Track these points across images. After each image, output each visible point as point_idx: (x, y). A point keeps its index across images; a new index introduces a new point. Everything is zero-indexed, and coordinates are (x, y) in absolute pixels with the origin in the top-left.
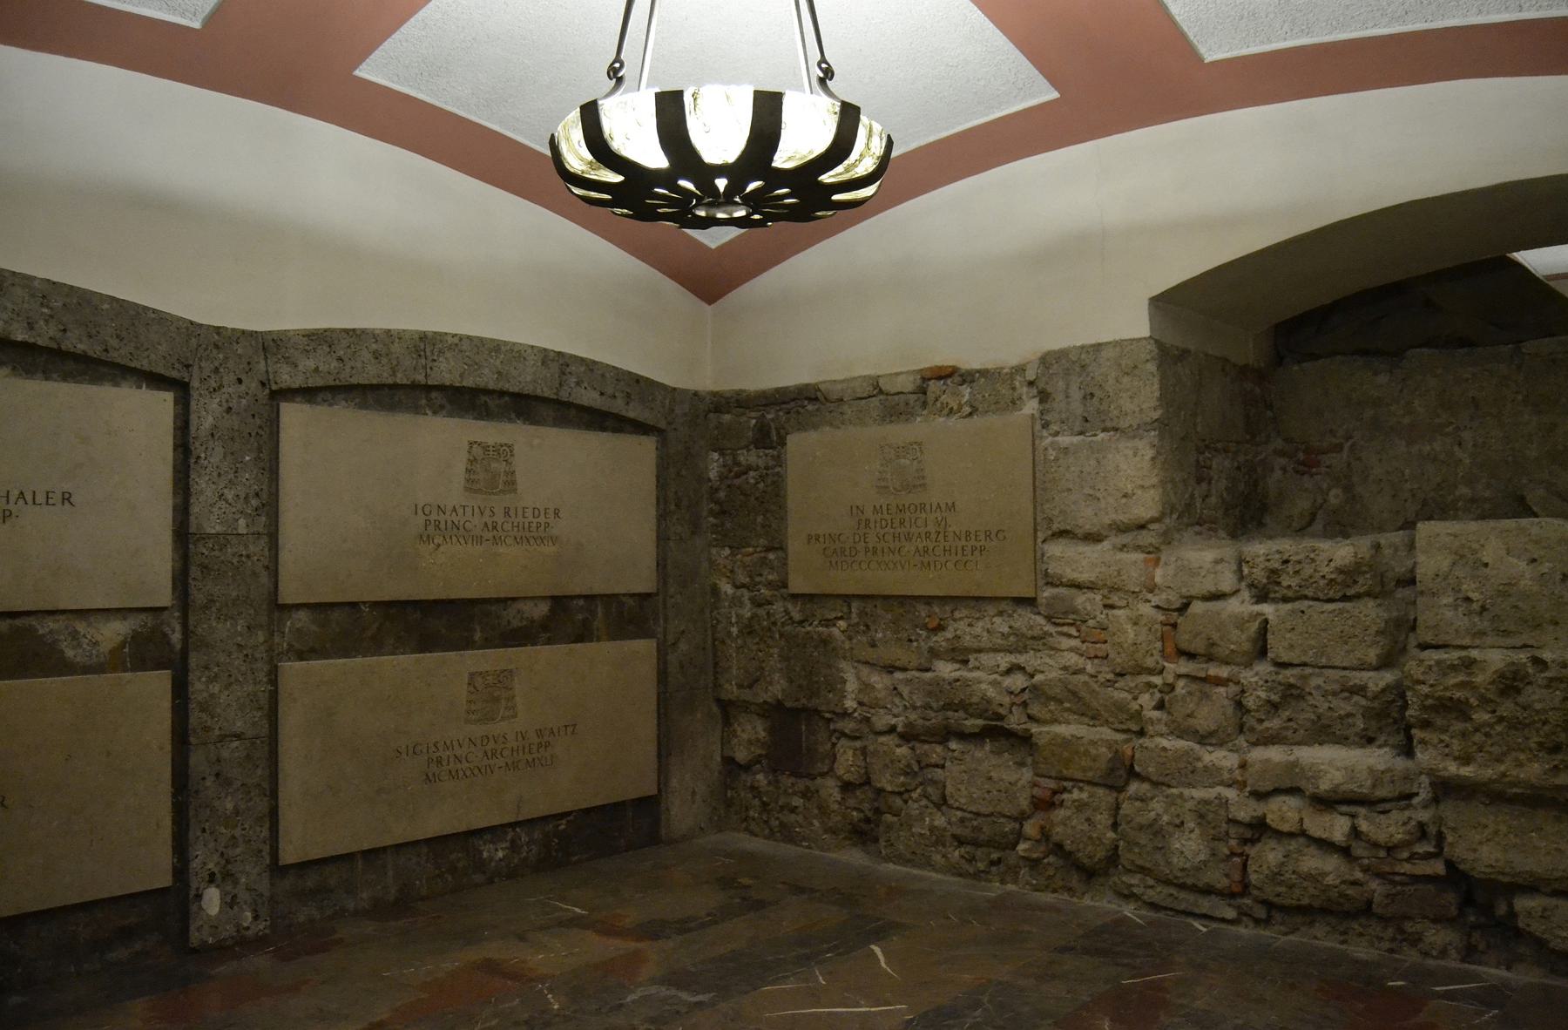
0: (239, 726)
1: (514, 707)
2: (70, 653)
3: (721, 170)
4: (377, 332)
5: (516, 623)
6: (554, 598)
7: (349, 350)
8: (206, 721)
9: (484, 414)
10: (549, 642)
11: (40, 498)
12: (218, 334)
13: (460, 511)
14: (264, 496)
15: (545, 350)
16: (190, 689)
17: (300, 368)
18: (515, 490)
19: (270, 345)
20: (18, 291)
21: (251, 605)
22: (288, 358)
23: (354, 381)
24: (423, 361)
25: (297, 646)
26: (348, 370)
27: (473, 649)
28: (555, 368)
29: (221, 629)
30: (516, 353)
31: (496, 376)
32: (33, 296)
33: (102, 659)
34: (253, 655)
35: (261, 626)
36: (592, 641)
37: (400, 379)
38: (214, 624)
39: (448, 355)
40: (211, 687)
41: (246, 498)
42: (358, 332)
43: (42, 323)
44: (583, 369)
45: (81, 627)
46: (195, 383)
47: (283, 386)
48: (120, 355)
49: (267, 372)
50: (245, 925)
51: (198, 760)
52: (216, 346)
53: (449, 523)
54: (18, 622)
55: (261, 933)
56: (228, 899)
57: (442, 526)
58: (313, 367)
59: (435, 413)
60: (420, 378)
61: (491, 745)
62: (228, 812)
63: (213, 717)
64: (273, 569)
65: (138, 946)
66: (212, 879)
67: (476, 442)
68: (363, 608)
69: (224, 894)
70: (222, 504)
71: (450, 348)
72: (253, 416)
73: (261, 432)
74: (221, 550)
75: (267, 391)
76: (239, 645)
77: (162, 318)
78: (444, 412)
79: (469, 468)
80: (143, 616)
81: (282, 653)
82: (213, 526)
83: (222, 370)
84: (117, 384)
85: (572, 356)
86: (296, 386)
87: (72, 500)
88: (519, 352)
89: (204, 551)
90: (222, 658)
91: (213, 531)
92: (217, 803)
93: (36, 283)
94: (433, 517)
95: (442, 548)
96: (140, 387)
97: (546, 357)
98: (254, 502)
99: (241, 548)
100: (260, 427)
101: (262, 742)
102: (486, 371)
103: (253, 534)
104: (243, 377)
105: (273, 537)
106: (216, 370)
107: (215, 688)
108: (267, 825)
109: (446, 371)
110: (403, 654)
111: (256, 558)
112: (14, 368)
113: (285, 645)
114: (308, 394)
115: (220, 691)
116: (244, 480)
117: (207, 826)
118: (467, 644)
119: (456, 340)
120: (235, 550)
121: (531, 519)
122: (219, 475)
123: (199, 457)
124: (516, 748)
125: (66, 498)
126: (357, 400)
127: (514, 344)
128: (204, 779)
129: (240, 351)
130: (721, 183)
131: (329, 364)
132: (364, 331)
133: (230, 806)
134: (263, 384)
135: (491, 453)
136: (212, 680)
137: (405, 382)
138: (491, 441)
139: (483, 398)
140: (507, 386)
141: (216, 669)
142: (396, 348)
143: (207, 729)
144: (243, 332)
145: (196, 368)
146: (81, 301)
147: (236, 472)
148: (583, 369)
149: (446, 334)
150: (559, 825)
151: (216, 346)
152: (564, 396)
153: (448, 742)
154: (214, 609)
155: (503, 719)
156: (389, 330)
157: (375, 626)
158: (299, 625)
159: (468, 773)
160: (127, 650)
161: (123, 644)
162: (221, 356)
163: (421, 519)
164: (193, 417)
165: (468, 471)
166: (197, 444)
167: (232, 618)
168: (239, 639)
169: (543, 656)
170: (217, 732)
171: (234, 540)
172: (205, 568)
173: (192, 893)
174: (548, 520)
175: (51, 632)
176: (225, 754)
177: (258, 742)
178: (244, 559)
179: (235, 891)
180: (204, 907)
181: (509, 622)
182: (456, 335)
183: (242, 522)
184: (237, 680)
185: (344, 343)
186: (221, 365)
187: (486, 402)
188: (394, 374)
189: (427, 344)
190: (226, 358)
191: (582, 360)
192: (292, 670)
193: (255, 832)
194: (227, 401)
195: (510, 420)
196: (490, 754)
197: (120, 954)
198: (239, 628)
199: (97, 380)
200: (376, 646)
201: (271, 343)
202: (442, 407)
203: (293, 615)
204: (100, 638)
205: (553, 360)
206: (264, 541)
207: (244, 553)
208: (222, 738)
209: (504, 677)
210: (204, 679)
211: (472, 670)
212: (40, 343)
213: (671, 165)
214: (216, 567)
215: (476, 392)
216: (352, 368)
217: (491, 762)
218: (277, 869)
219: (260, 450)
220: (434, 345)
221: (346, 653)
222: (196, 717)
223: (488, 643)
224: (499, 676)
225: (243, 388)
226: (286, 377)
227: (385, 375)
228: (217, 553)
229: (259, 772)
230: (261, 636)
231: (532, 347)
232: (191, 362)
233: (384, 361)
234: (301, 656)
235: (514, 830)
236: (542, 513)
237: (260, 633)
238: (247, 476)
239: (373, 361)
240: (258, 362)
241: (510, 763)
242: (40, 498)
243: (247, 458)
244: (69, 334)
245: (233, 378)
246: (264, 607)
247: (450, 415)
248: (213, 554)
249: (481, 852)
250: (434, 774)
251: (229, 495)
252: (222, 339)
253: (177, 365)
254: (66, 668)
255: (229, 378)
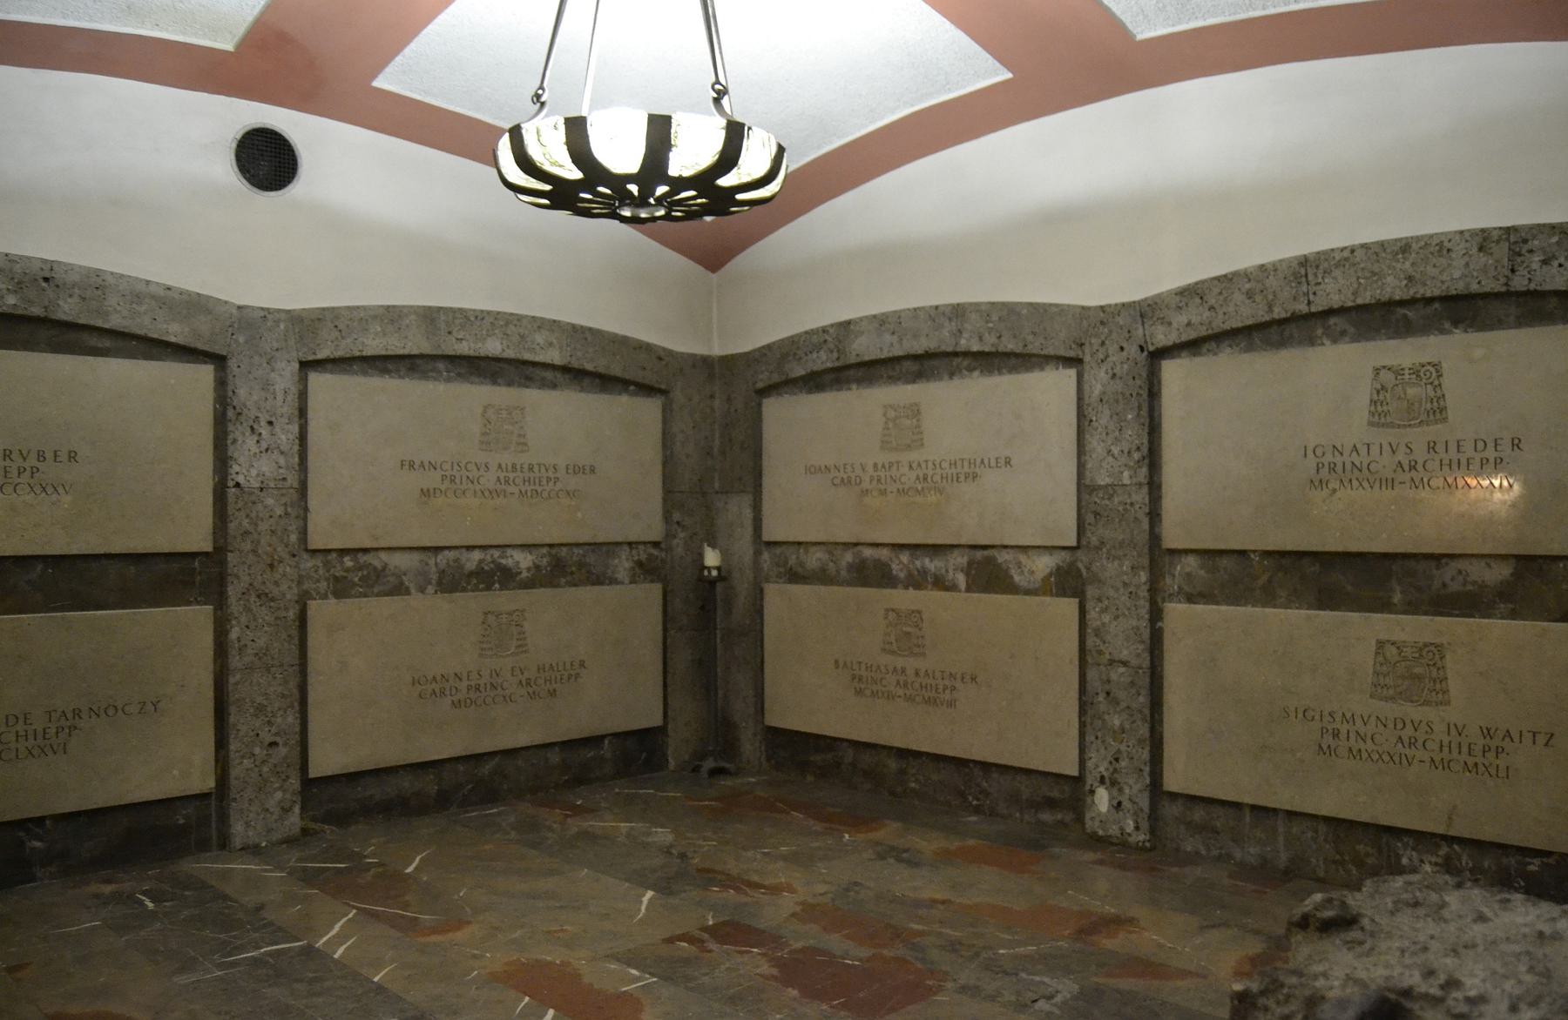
0: (1124, 654)
1: (1445, 692)
2: (1017, 578)
3: (629, 178)
4: (1249, 271)
5: (1455, 587)
6: (1518, 557)
7: (1221, 298)
8: (1099, 646)
9: (1405, 329)
10: (1514, 615)
11: (993, 463)
12: (1104, 312)
13: (1363, 451)
14: (1145, 450)
15: (1483, 231)
16: (1088, 617)
17: (1175, 325)
18: (1445, 420)
19: (1146, 311)
20: (974, 316)
21: (1134, 548)
22: (1163, 318)
23: (1227, 326)
24: (1304, 288)
25: (1186, 588)
26: (1221, 316)
27: (1390, 612)
28: (1501, 252)
29: (1111, 568)
30: (1439, 247)
31: (1405, 282)
32: (981, 316)
33: (1037, 586)
34: (1136, 593)
35: (1144, 568)
36: (926, 588)
37: (1278, 313)
38: (1105, 563)
39: (1337, 273)
40: (1103, 617)
41: (1129, 452)
42: (1230, 276)
43: (987, 335)
44: (1555, 239)
45: (1023, 558)
46: (1087, 358)
47: (1160, 345)
48: (1034, 348)
49: (1145, 335)
50: (1128, 831)
51: (1092, 674)
52: (1102, 323)
53: (1348, 467)
54: (986, 553)
55: (1140, 844)
56: (1115, 803)
57: (1339, 468)
58: (1186, 321)
59: (1335, 341)
60: (1302, 307)
61: (1409, 731)
62: (1116, 728)
63: (1104, 643)
64: (1154, 515)
65: (1059, 817)
66: (1102, 780)
67: (1384, 367)
68: (1252, 556)
69: (1111, 798)
70: (1110, 459)
71: (1337, 266)
72: (1134, 378)
73: (1141, 392)
74: (1109, 499)
75: (1146, 353)
76: (1125, 584)
77: (1062, 309)
78: (1347, 339)
79: (1375, 397)
80: (1063, 553)
81: (1173, 594)
82: (1103, 479)
83: (1107, 342)
84: (1042, 369)
85: (1532, 227)
86: (1171, 343)
87: (1521, 446)
88: (1441, 244)
89: (1096, 500)
90: (1111, 593)
91: (1102, 483)
92: (1106, 717)
93: (983, 308)
94: (1329, 458)
95: (1338, 494)
96: (1057, 369)
97: (1484, 240)
98: (1136, 456)
99: (1126, 496)
100: (1140, 387)
101: (1144, 672)
102: (1389, 279)
103: (1136, 484)
104: (1125, 345)
105: (1154, 487)
106: (1103, 343)
107: (1106, 618)
108: (1148, 748)
109: (1333, 292)
110: (1297, 608)
111: (1138, 506)
112: (981, 372)
113: (1176, 587)
114: (1193, 346)
115: (1110, 622)
116: (1127, 436)
117: (1099, 734)
118: (1385, 606)
119: (1346, 254)
120: (1121, 499)
121: (1470, 452)
122: (1107, 434)
123: (1091, 421)
124: (1445, 743)
125: (1008, 462)
126: (1242, 345)
127: (1431, 236)
128: (1097, 694)
129: (1121, 323)
130: (633, 188)
131: (1201, 315)
132: (1236, 274)
133: (1117, 722)
134: (1142, 349)
135: (1407, 376)
136: (1105, 610)
137: (1283, 315)
138: (1407, 362)
139: (1401, 311)
140: (1422, 291)
141: (1106, 603)
142: (1272, 282)
143: (1100, 652)
144: (1123, 305)
145: (1087, 344)
146: (1010, 311)
147: (1120, 430)
148: (1555, 239)
149: (1333, 250)
150: (1530, 864)
151: (1102, 323)
152: (1519, 283)
153: (1348, 715)
154: (1104, 550)
155: (1426, 703)
156: (1263, 265)
157: (1265, 578)
158: (1188, 570)
159: (1375, 757)
160: (1053, 579)
161: (1050, 574)
162: (1106, 330)
163: (1311, 462)
164: (1086, 387)
165: (1373, 402)
166: (1090, 409)
167: (1120, 559)
168: (1125, 577)
169: (1498, 631)
170: (1108, 656)
171: (1120, 491)
172: (1096, 514)
173: (1087, 787)
174: (1502, 455)
175: (1006, 561)
176: (1114, 676)
177: (1141, 671)
178: (1128, 507)
179: (1120, 798)
180: (1096, 802)
181: (1444, 585)
182: (1346, 248)
183: (1126, 474)
184: (1124, 614)
185: (1216, 290)
186: (1106, 338)
187: (1405, 316)
188: (1270, 308)
189: (1306, 268)
190: (1111, 332)
191: (1553, 227)
192: (1176, 611)
193: (1137, 751)
194: (1112, 369)
195: (1443, 332)
196: (1406, 741)
197: (1046, 816)
198: (1125, 568)
199: (1029, 369)
200: (1268, 598)
201: (1147, 309)
202: (1343, 333)
203: (1183, 560)
204: (1034, 568)
205: (1498, 242)
206: (1145, 490)
207: (1129, 501)
208: (1112, 662)
209: (1433, 652)
210: (1097, 609)
211: (1383, 636)
212: (987, 350)
213: (669, 176)
214: (1106, 514)
215: (1390, 305)
216: (1225, 314)
217: (1407, 751)
218: (1156, 786)
219: (1140, 408)
220: (1317, 267)
221: (1235, 600)
222: (1091, 641)
223: (1412, 608)
224: (1421, 649)
225: (1125, 353)
226: (1161, 337)
227: (1261, 313)
228: (1107, 502)
229: (1141, 699)
230: (1143, 576)
231: (1462, 232)
232: (1083, 341)
233: (1258, 298)
234: (1191, 599)
235: (1450, 846)
236: (1491, 445)
237: (1142, 573)
238: (1130, 433)
239: (1247, 301)
240: (1136, 329)
241: (1437, 759)
242: (993, 463)
243: (1130, 416)
244: (1003, 339)
245: (1116, 347)
246: (1146, 550)
247: (1355, 339)
248: (1103, 502)
249: (1398, 857)
250: (1329, 746)
251: (1116, 450)
252: (1106, 315)
253: (1073, 346)
254: (1012, 589)
255: (1112, 348)
